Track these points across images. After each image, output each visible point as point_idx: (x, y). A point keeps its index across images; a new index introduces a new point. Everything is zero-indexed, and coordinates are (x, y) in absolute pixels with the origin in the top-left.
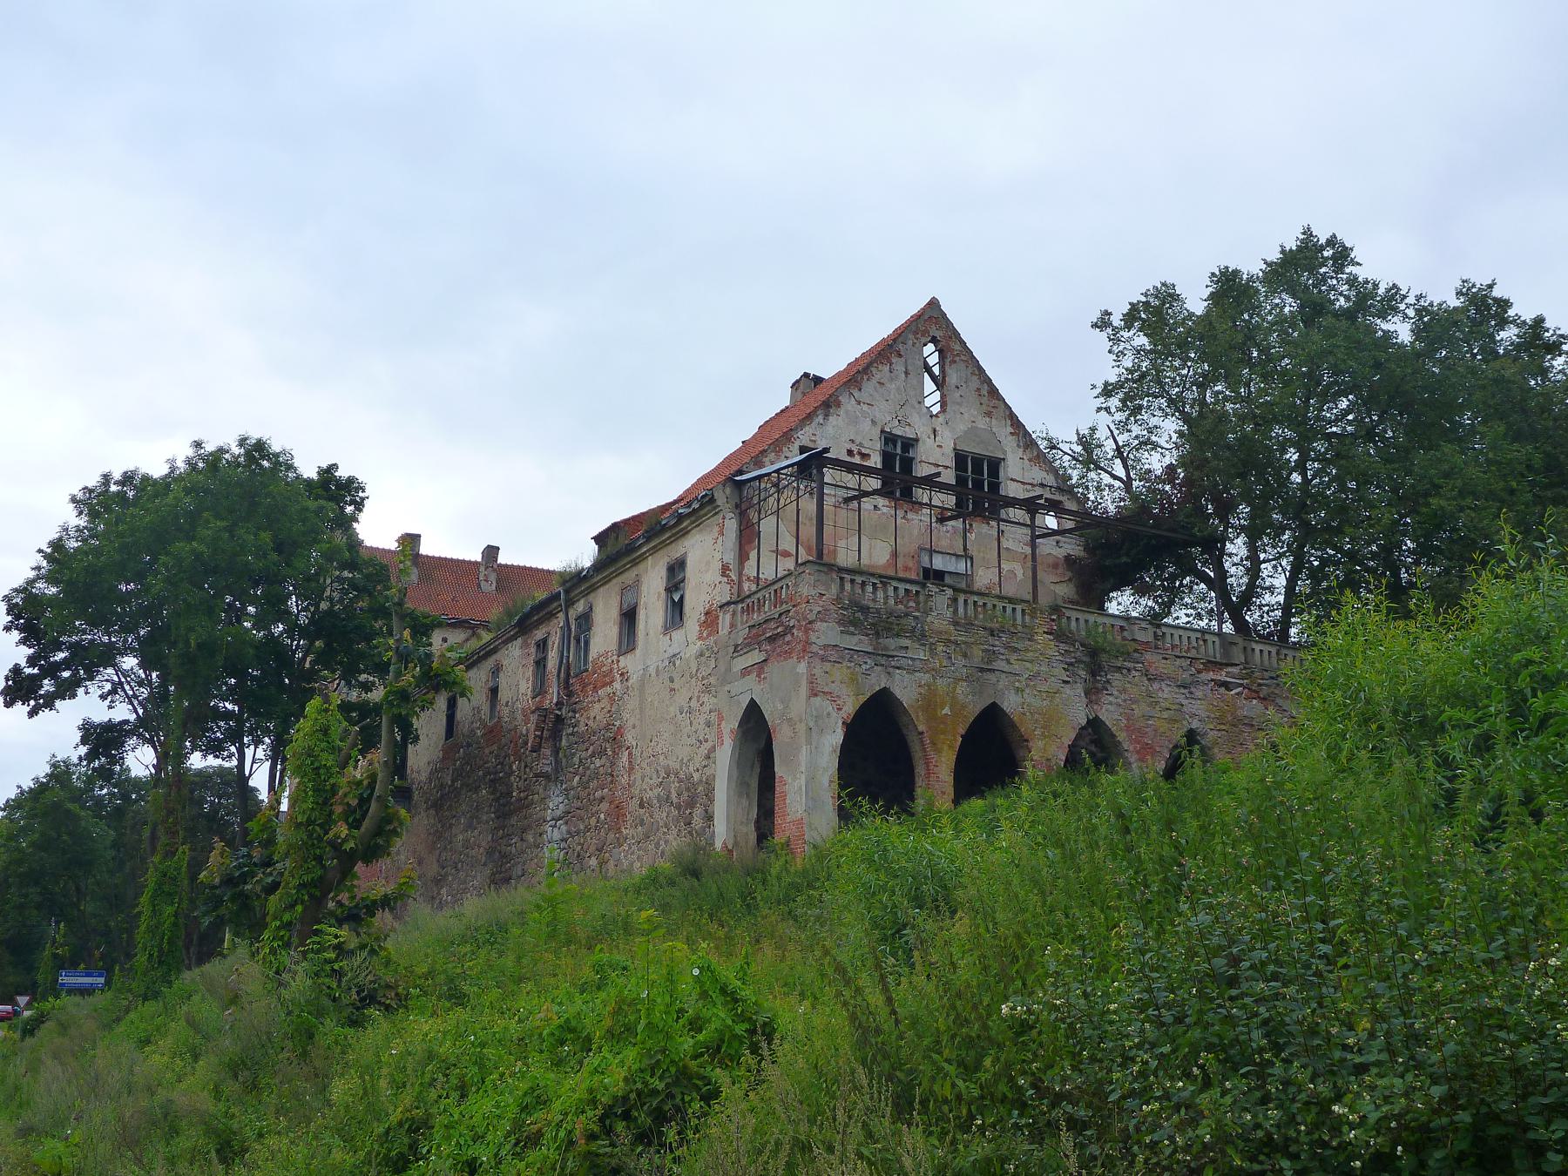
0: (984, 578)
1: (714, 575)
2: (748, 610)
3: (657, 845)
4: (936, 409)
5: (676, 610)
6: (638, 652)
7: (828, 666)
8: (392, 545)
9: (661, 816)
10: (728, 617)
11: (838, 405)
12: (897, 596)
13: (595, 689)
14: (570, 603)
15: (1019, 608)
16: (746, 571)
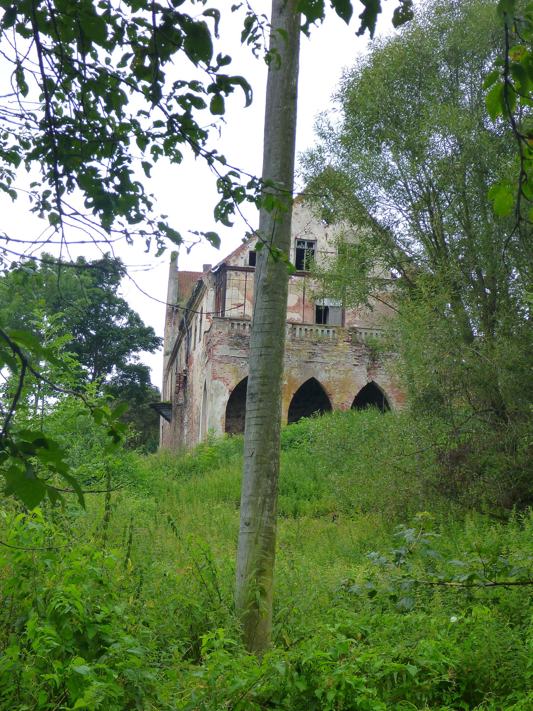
7: (222, 365)
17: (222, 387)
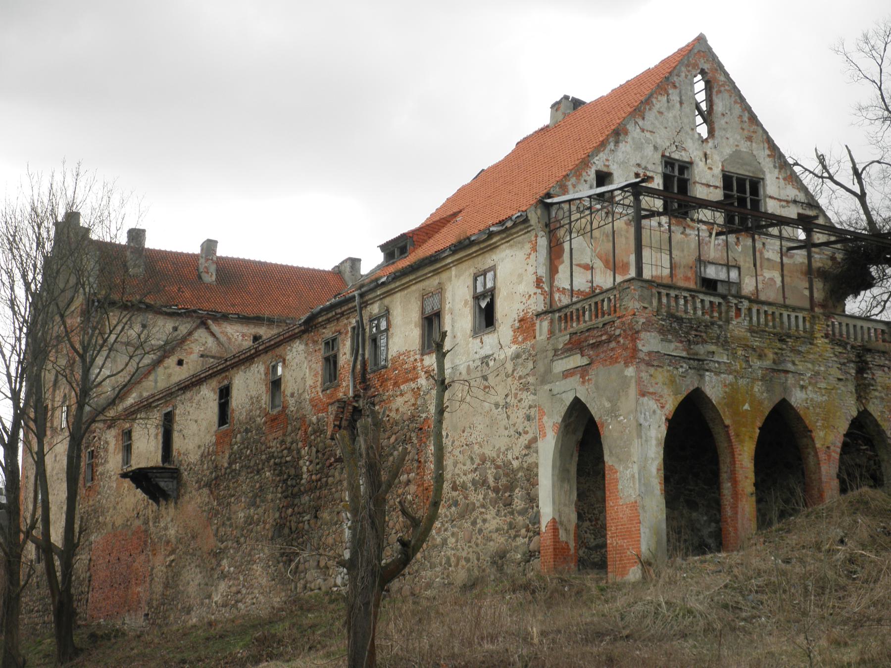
0: (748, 286)
1: (527, 286)
2: (567, 319)
3: (474, 523)
4: (705, 135)
5: (487, 317)
7: (652, 370)
8: (197, 250)
9: (477, 497)
10: (546, 324)
11: (626, 133)
12: (703, 307)
13: (396, 384)
14: (364, 304)
15: (801, 315)
16: (556, 283)
17: (654, 412)
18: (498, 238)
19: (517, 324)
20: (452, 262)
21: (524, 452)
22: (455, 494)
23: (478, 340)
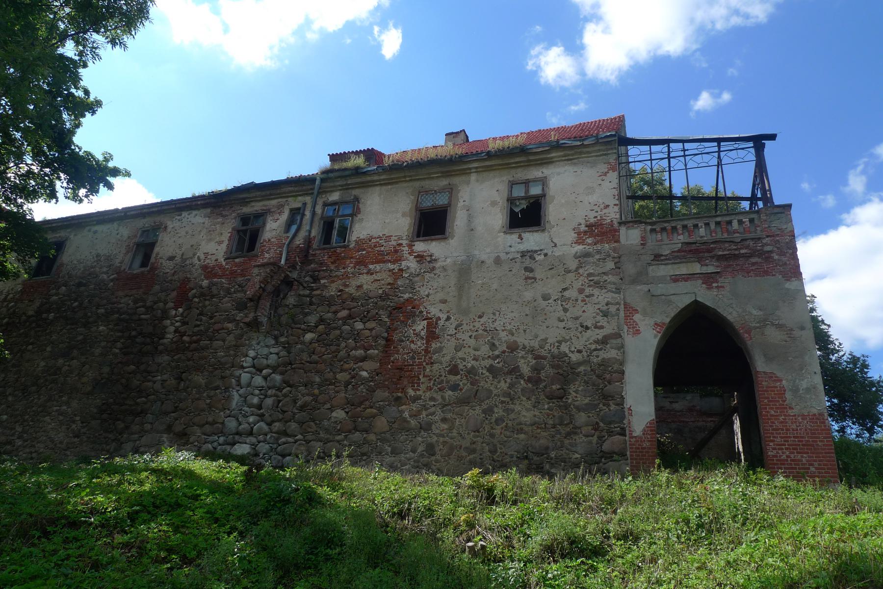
3: (489, 411)
6: (453, 242)
18: (562, 153)
19: (583, 228)
20: (476, 168)
21: (593, 347)
22: (452, 378)
23: (515, 237)
